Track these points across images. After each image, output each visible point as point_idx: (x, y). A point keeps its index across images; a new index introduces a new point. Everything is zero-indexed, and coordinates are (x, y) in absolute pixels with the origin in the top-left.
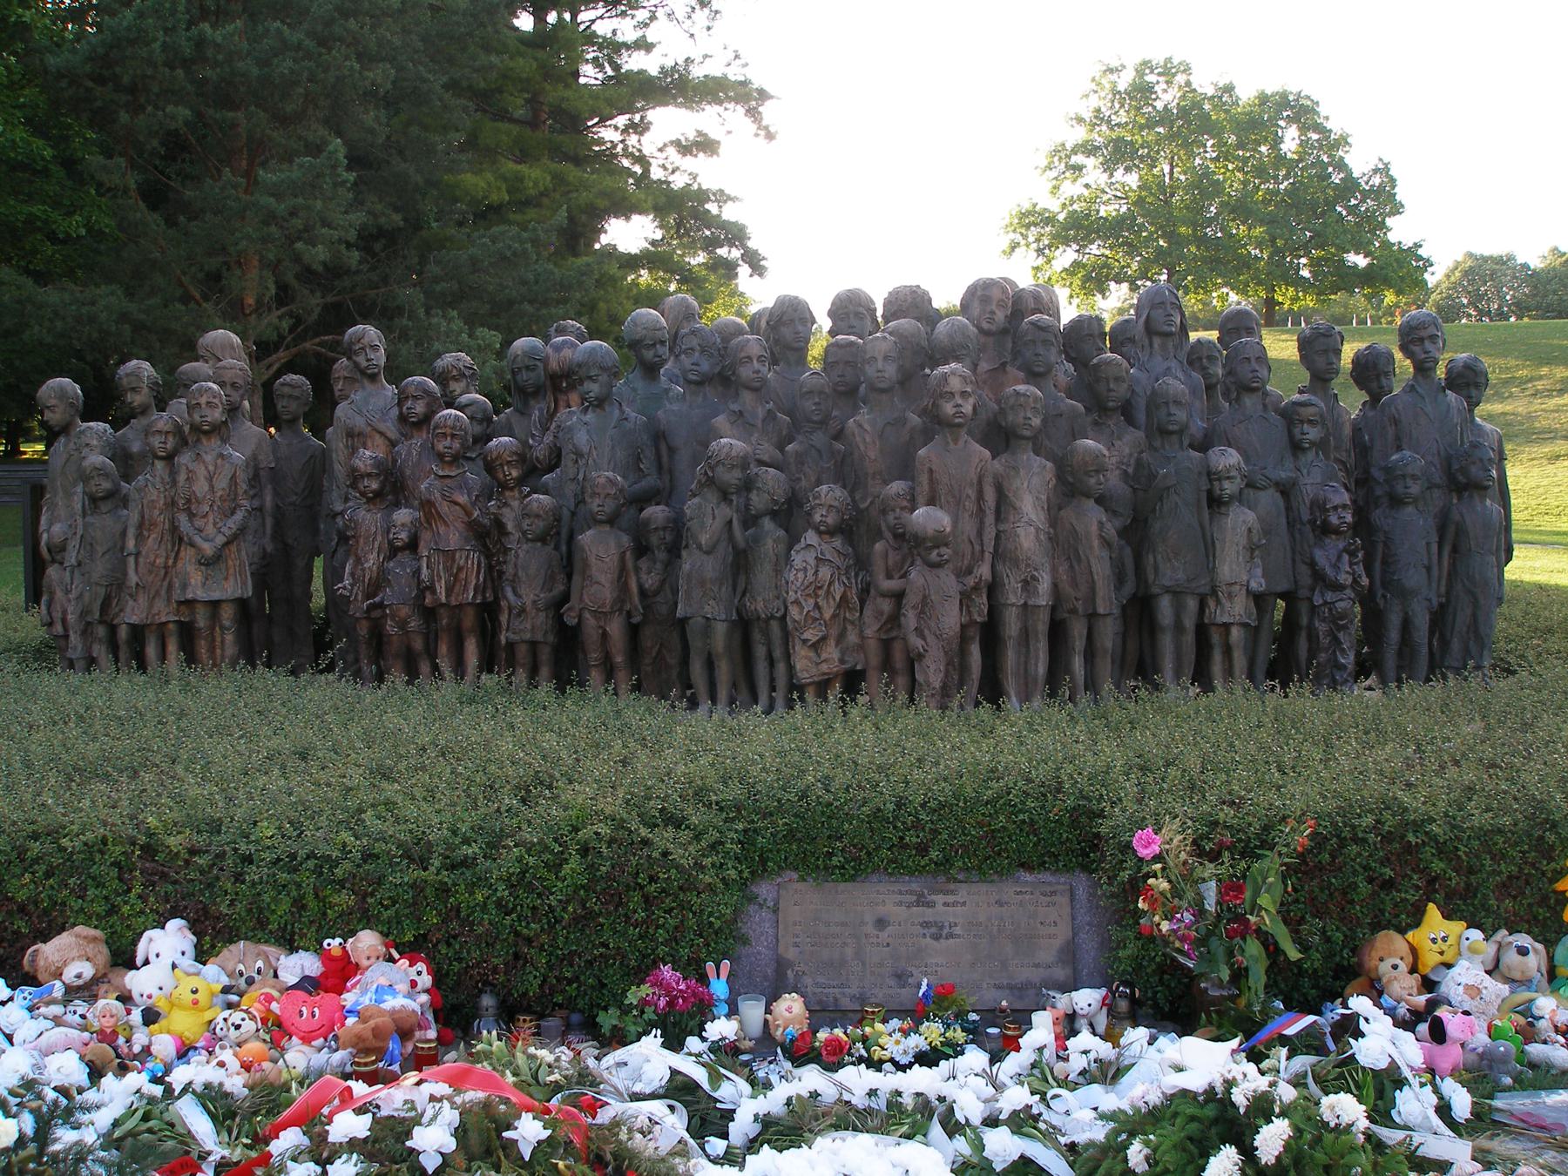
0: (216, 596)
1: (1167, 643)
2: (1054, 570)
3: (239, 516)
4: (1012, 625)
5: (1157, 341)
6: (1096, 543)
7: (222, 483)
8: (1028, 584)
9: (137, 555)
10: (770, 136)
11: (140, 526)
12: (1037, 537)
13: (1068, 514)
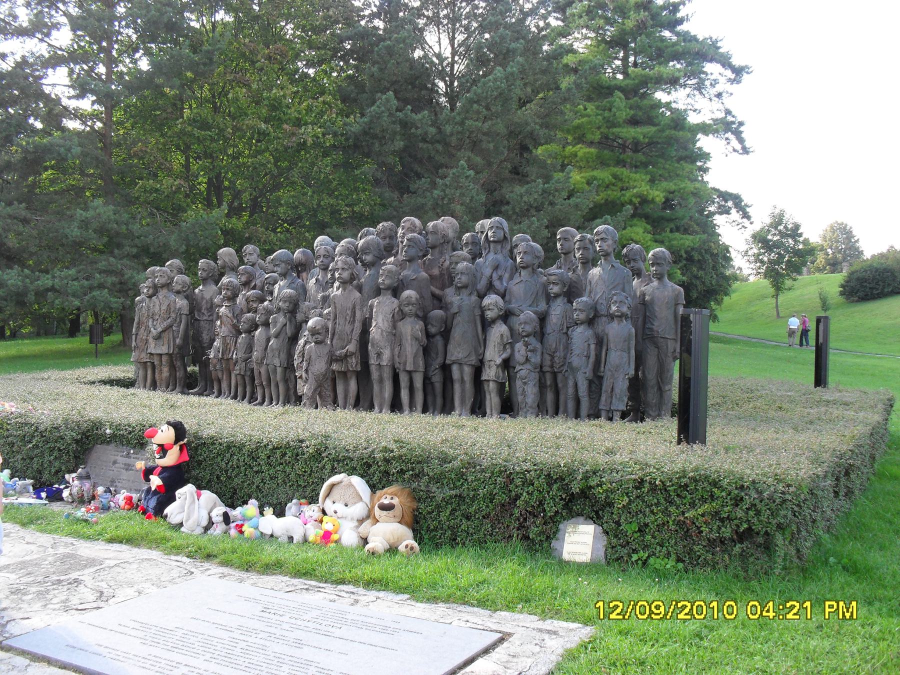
0: (159, 352)
1: (457, 387)
2: (392, 350)
3: (169, 320)
4: (375, 375)
5: (492, 245)
6: (409, 338)
7: (164, 307)
8: (379, 355)
9: (137, 334)
10: (745, 151)
11: (138, 323)
12: (382, 334)
13: (400, 324)
